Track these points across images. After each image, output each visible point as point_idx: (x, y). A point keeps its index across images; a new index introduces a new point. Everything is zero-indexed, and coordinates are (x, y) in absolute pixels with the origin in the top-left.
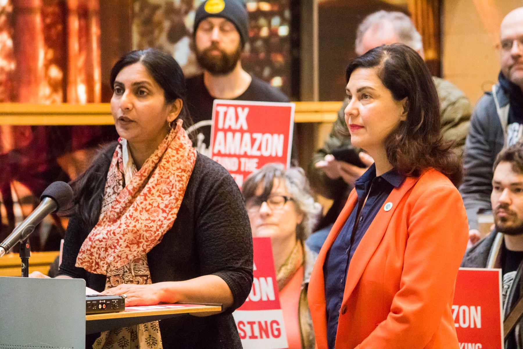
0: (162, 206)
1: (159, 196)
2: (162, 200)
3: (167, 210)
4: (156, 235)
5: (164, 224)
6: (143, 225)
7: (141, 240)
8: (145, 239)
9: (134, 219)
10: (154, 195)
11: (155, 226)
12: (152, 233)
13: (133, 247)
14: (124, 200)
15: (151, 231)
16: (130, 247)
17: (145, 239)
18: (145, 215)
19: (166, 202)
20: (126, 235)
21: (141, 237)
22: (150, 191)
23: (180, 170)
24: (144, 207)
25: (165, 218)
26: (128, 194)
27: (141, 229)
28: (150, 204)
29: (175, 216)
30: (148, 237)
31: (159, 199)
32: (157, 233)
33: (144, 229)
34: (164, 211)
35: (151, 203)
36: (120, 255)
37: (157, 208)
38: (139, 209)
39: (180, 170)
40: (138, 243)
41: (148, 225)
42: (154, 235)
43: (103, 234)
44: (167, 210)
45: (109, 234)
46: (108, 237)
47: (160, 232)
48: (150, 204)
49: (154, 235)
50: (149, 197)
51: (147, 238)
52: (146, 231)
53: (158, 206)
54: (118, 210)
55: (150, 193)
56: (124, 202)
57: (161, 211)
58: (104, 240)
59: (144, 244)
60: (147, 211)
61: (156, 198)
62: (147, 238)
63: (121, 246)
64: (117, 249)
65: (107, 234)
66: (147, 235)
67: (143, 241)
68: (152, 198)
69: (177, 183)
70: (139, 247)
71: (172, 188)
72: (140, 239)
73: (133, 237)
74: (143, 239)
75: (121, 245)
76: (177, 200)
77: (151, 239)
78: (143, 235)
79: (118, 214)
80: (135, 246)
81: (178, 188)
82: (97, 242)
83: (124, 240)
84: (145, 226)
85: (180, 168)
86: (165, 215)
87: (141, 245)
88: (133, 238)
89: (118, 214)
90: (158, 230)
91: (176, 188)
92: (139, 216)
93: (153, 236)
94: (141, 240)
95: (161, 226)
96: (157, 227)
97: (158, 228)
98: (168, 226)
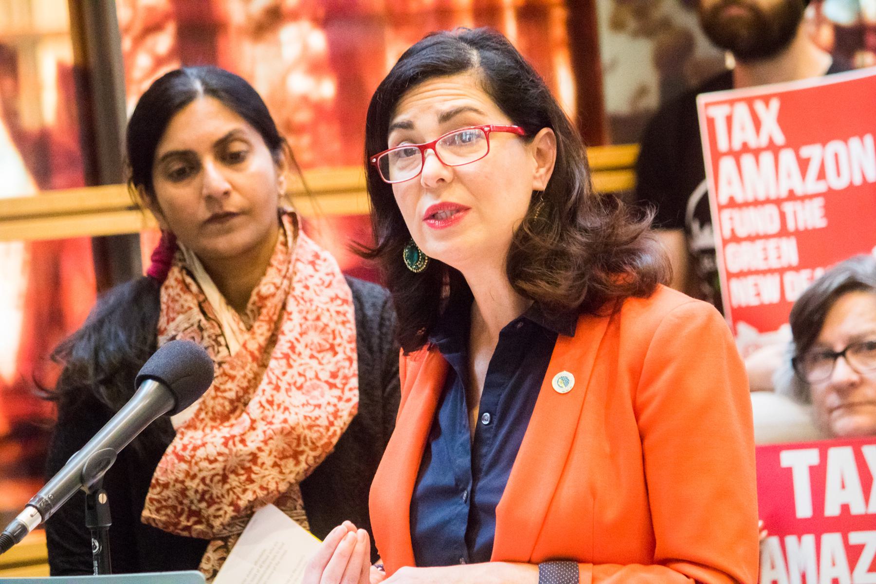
0: (325, 376)
1: (312, 357)
2: (320, 363)
3: (338, 382)
4: (330, 433)
5: (342, 410)
6: (301, 417)
7: (302, 448)
8: (310, 444)
9: (279, 406)
10: (303, 356)
11: (324, 415)
12: (321, 430)
13: (286, 466)
14: (242, 373)
15: (318, 426)
16: (279, 466)
17: (310, 444)
18: (298, 398)
19: (331, 368)
20: (271, 442)
21: (302, 441)
22: (293, 348)
23: (339, 302)
24: (291, 381)
25: (340, 399)
26: (250, 359)
27: (298, 424)
28: (300, 375)
29: (357, 392)
30: (316, 439)
31: (314, 363)
32: (332, 429)
33: (305, 423)
34: (332, 386)
35: (302, 372)
36: (265, 486)
37: (315, 381)
38: (283, 385)
39: (339, 302)
40: (296, 455)
41: (310, 415)
42: (327, 433)
43: (216, 446)
44: (338, 382)
45: (230, 443)
46: (231, 450)
47: (337, 426)
48: (300, 375)
49: (327, 433)
50: (295, 361)
51: (313, 443)
52: (310, 427)
53: (317, 377)
54: (232, 395)
55: (294, 352)
56: (245, 376)
57: (326, 387)
58: (220, 459)
59: (308, 456)
60: (300, 388)
61: (307, 360)
62: (313, 443)
63: (265, 466)
64: (256, 474)
65: (225, 444)
66: (312, 435)
67: (307, 449)
68: (299, 361)
69: (340, 327)
70: (298, 463)
71: (334, 338)
72: (298, 445)
73: (286, 443)
74: (306, 445)
75: (263, 464)
76: (350, 359)
77: (323, 442)
78: (305, 437)
79: (231, 402)
80: (291, 462)
81: (345, 337)
82: (204, 464)
83: (267, 452)
84: (305, 417)
85: (337, 297)
86: (337, 392)
87: (302, 458)
88: (286, 446)
89: (231, 402)
90: (332, 424)
91: (342, 337)
92: (287, 399)
93: (324, 436)
94: (302, 448)
95: (336, 414)
96: (328, 418)
97: (331, 419)
98: (350, 414)
